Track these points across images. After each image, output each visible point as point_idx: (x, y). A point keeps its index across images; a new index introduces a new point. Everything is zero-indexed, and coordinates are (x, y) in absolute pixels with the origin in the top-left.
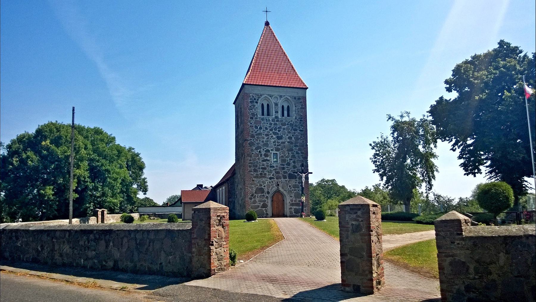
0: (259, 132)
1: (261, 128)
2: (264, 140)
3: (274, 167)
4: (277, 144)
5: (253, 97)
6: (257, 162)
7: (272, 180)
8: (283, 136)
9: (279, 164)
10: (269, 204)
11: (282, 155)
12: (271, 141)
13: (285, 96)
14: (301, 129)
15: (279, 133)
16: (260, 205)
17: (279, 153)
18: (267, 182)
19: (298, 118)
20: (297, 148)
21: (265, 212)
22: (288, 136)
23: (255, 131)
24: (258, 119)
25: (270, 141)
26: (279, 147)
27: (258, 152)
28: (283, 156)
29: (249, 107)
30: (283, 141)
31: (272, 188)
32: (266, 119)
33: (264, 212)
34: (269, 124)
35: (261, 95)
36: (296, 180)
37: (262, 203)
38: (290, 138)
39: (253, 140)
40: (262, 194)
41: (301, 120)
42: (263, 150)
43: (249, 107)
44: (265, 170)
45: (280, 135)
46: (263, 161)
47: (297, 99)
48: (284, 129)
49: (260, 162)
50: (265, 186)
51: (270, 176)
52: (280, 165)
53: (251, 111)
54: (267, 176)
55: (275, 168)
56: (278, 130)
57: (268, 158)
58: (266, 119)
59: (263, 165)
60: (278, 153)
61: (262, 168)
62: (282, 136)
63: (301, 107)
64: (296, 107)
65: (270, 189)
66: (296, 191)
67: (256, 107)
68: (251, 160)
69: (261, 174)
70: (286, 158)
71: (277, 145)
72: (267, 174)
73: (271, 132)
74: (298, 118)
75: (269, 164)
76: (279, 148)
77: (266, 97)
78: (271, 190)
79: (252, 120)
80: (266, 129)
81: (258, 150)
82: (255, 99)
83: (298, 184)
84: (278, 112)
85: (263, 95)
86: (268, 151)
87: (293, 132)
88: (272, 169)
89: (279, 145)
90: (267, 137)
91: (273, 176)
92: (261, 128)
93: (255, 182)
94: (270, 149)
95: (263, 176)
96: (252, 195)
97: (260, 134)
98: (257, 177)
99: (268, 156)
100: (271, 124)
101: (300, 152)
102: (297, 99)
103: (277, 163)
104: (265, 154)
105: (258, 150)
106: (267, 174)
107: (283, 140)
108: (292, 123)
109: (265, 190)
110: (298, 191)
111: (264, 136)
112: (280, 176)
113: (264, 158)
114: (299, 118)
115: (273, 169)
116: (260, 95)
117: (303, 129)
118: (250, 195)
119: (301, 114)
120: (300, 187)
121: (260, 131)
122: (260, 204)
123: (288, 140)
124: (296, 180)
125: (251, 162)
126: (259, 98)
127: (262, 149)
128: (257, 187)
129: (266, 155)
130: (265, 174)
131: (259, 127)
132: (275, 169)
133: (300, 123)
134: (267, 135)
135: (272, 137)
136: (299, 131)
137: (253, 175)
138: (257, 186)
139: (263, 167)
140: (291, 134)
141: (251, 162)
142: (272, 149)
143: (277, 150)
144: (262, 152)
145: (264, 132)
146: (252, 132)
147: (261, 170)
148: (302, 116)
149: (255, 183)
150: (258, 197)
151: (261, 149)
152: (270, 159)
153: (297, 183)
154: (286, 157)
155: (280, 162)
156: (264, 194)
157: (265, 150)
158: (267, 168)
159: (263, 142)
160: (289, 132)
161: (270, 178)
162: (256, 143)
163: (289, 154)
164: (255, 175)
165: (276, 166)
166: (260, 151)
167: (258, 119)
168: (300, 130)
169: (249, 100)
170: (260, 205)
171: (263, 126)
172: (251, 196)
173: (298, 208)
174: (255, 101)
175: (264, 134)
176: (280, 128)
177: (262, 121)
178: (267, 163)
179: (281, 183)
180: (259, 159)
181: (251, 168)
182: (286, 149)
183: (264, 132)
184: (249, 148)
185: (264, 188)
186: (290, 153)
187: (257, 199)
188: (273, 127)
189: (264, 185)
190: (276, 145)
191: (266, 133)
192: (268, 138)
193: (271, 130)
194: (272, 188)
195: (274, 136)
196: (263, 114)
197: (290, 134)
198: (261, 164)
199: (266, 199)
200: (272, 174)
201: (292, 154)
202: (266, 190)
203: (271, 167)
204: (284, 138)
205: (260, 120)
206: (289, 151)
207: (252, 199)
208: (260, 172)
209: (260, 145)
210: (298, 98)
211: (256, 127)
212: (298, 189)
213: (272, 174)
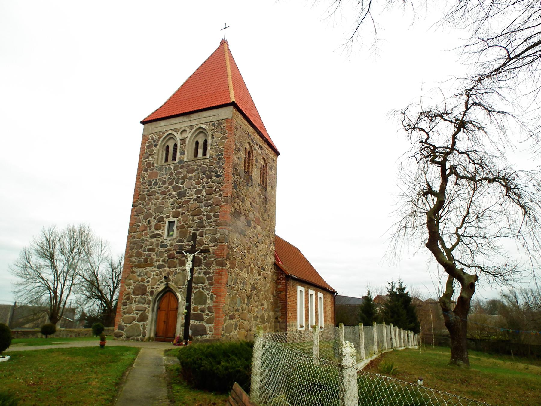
0: (153, 190)
1: (156, 183)
2: (158, 202)
3: (166, 246)
4: (176, 205)
5: (153, 138)
6: (143, 239)
7: (160, 270)
8: (188, 189)
9: (175, 241)
10: (150, 316)
11: (182, 223)
12: (169, 201)
13: (197, 125)
14: (219, 173)
15: (182, 187)
16: (136, 316)
17: (178, 220)
18: (153, 273)
19: (214, 157)
20: (209, 208)
21: (142, 329)
22: (195, 190)
23: (148, 189)
24: (154, 171)
25: (167, 202)
26: (180, 210)
27: (147, 223)
28: (183, 225)
29: (145, 154)
30: (187, 199)
31: (159, 285)
32: (166, 168)
33: (141, 331)
34: (168, 174)
35: (163, 134)
36: (200, 267)
37: (141, 312)
38: (199, 192)
39: (143, 204)
40: (143, 297)
41: (219, 159)
42: (154, 218)
43: (145, 154)
44: (154, 253)
45: (182, 190)
46: (152, 237)
47: (216, 125)
48: (191, 178)
49: (148, 239)
50: (148, 282)
51: (158, 263)
52: (177, 242)
53: (147, 160)
54: (155, 263)
55: (168, 247)
56: (180, 181)
57: (160, 232)
58: (166, 168)
59: (152, 244)
60: (175, 220)
61: (149, 250)
62: (186, 190)
63: (222, 136)
64: (213, 138)
65: (155, 287)
66: (197, 290)
67: (154, 153)
68: (134, 238)
69: (146, 260)
70: (189, 229)
71: (177, 207)
72: (155, 258)
73: (170, 187)
74: (214, 157)
75: (161, 241)
76: (178, 211)
77: (170, 134)
78: (157, 288)
79: (146, 173)
80: (164, 183)
81: (148, 220)
82: (154, 141)
83: (204, 276)
84: (184, 154)
85: (166, 132)
86: (161, 220)
87: (205, 180)
88: (162, 249)
89: (180, 207)
90: (163, 196)
91: (163, 263)
92: (156, 183)
93: (136, 275)
94: (165, 216)
95: (149, 264)
96: (128, 299)
97: (154, 193)
98: (139, 266)
99: (160, 229)
100: (171, 174)
101: (212, 215)
102: (216, 125)
103: (172, 238)
104: (156, 225)
105: (148, 220)
106: (155, 258)
107: (186, 198)
108: (205, 166)
109: (148, 288)
110: (201, 289)
111: (158, 195)
112: (174, 262)
113: (154, 232)
114: (217, 156)
115: (164, 251)
116: (161, 133)
117: (222, 172)
118: (125, 297)
119: (222, 148)
120: (206, 281)
121: (154, 188)
122: (137, 314)
123: (195, 196)
124: (200, 269)
125: (134, 240)
126: (160, 138)
127: (153, 217)
128: (137, 283)
129: (157, 227)
130: (152, 259)
131: (153, 182)
132: (169, 251)
133: (218, 163)
134: (163, 193)
135: (170, 194)
136: (214, 178)
137: (134, 262)
138: (137, 281)
139: (151, 247)
140: (201, 185)
141: (134, 240)
142: (168, 214)
143: (176, 215)
144: (153, 222)
145: (159, 189)
146: (144, 191)
147: (147, 253)
148: (222, 150)
149: (135, 276)
150: (135, 301)
151: (151, 218)
152: (162, 233)
153: (202, 275)
154: (189, 227)
155: (178, 236)
156: (146, 297)
157: (157, 218)
158: (157, 249)
159: (156, 204)
160: (198, 183)
161: (159, 267)
162: (146, 208)
163: (193, 220)
164: (136, 261)
165: (171, 245)
166: (149, 221)
167: (154, 171)
168: (218, 176)
169: (147, 144)
170: (136, 316)
171: (159, 179)
172: (126, 299)
173: (198, 324)
174: (154, 144)
175: (159, 192)
176: (185, 177)
177: (159, 172)
178: (157, 241)
179: (174, 275)
180: (146, 235)
181: (133, 251)
182: (189, 212)
183: (159, 189)
184: (136, 217)
185: (146, 284)
186: (196, 218)
187: (134, 304)
188: (174, 179)
189: (149, 279)
190: (174, 208)
191: (162, 189)
192: (164, 198)
193: (171, 184)
194: (159, 285)
195: (174, 193)
196: (166, 161)
197: (199, 185)
198: (148, 243)
199: (147, 305)
200: (162, 259)
201: (199, 220)
202: (149, 289)
203: (161, 246)
204: (188, 193)
205: (156, 171)
206: (195, 216)
207: (126, 305)
208: (146, 257)
209: (151, 211)
210: (218, 124)
211: (150, 183)
212: (203, 285)
213: (162, 259)
